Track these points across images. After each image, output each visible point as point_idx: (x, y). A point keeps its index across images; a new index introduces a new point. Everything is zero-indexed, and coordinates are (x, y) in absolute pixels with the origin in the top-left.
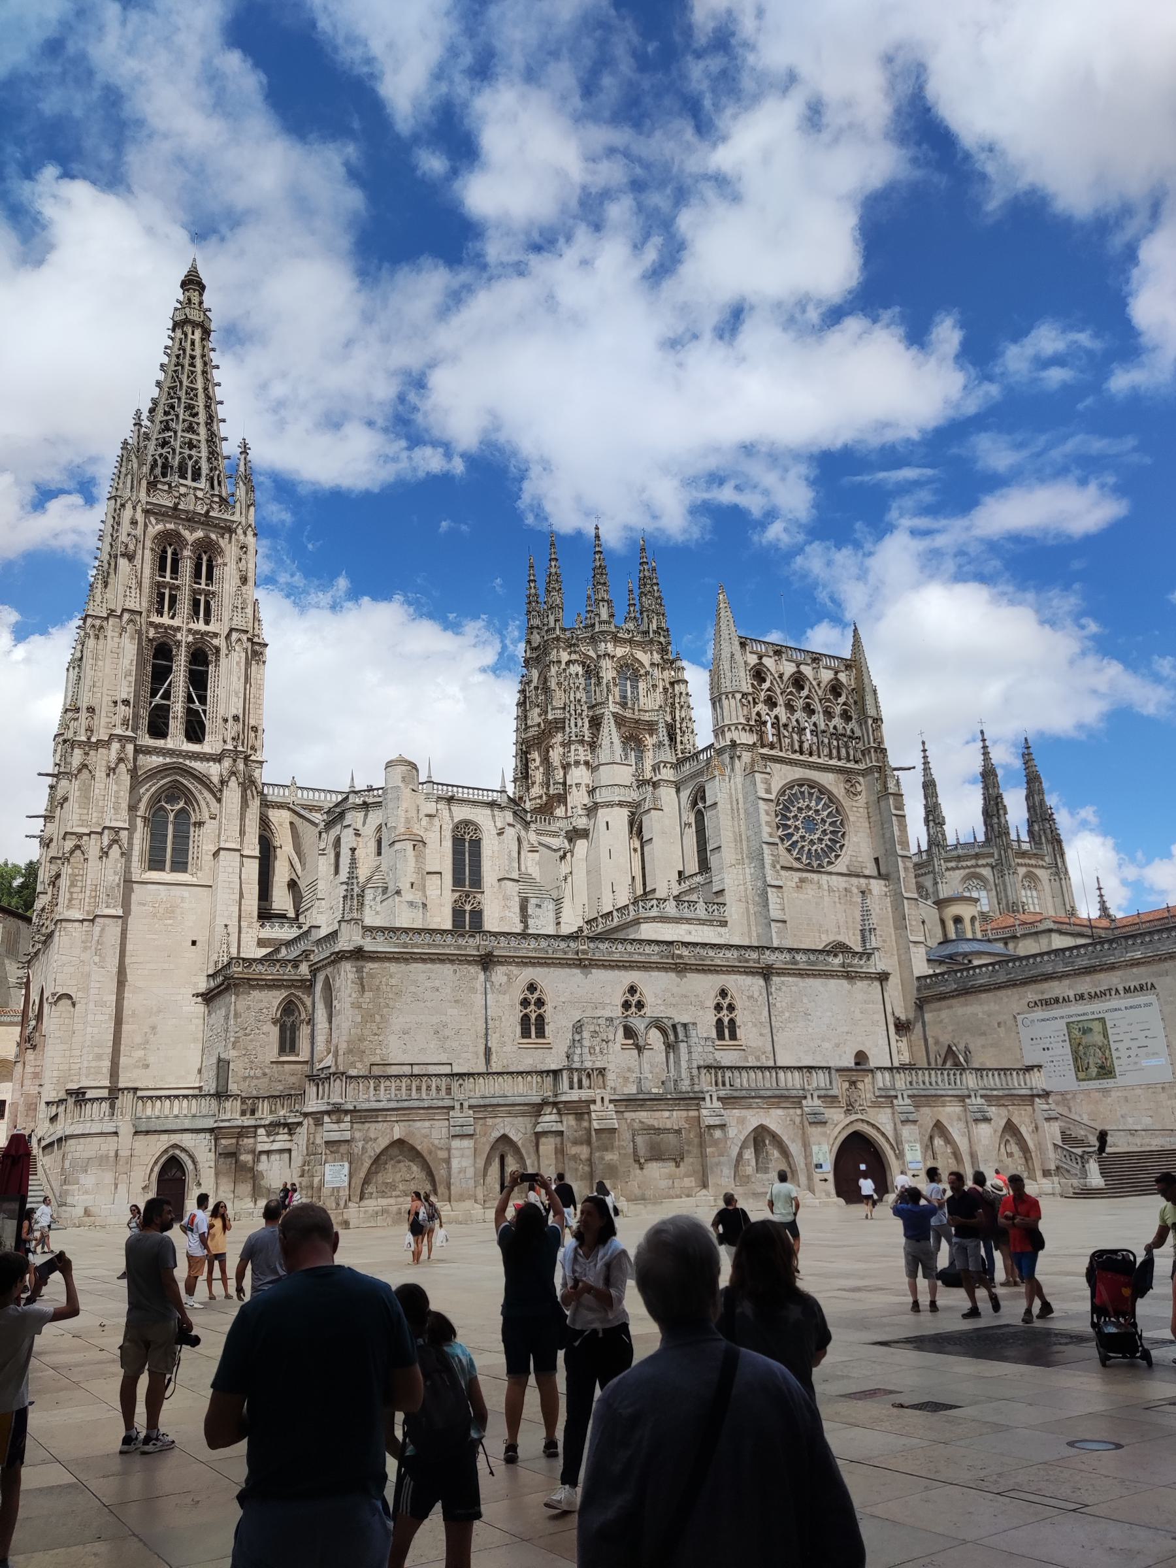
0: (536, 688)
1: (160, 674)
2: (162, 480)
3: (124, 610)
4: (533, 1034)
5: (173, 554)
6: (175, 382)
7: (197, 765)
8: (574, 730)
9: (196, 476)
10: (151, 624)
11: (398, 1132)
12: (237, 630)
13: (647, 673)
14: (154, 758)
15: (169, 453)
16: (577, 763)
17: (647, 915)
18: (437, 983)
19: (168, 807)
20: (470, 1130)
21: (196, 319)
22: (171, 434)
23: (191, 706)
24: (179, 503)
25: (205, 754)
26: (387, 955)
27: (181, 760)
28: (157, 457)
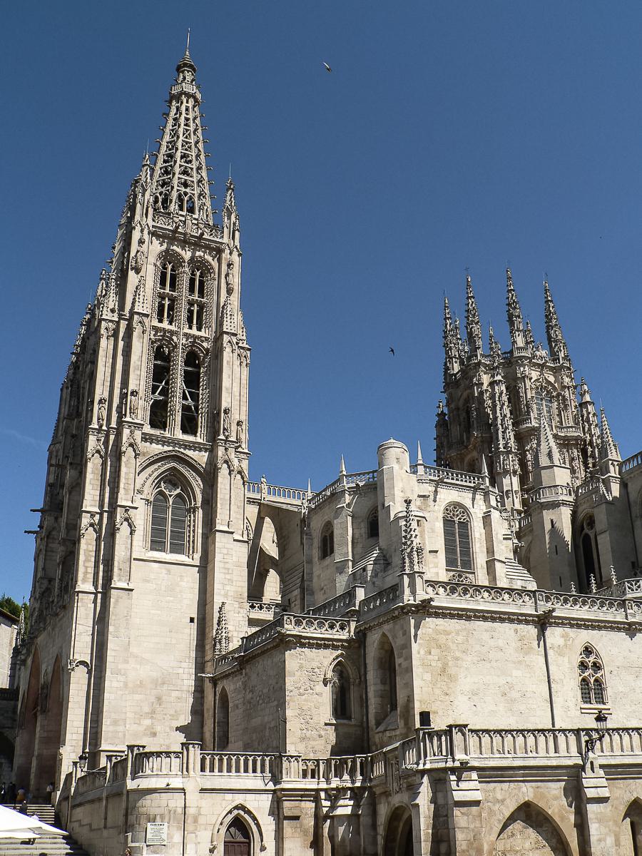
0: (458, 409)
1: (161, 373)
2: (162, 210)
3: (132, 313)
4: (593, 701)
6: (172, 137)
7: (190, 453)
8: (501, 442)
9: (191, 210)
10: (154, 328)
11: (527, 792)
12: (227, 333)
13: (559, 395)
15: (168, 190)
16: (506, 472)
17: (635, 595)
18: (501, 643)
19: (167, 493)
20: (604, 793)
27: (177, 449)
28: (158, 195)
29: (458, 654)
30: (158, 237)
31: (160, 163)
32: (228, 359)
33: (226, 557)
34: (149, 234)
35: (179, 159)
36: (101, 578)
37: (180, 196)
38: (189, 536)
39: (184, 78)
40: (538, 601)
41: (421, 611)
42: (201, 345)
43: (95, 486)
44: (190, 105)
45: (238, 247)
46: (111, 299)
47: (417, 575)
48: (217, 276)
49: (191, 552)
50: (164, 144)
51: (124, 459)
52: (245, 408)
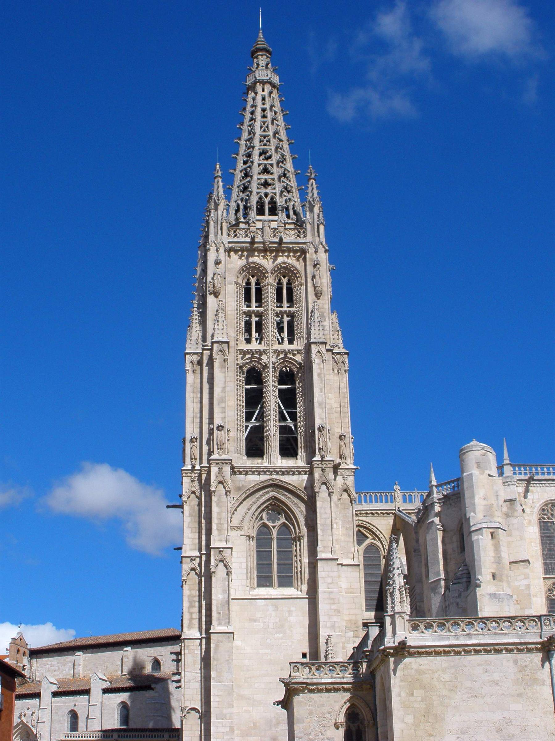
3: (213, 343)
5: (256, 284)
10: (241, 351)
14: (251, 477)
15: (247, 196)
19: (270, 524)
21: (265, 78)
22: (249, 179)
23: (283, 424)
24: (254, 237)
25: (298, 467)
26: (437, 649)
27: (275, 477)
28: (239, 202)
29: (445, 693)
30: (236, 251)
31: (240, 165)
32: (319, 371)
33: (330, 586)
34: (225, 251)
35: (257, 157)
36: (204, 623)
37: (261, 198)
38: (297, 567)
39: (258, 65)
40: (544, 627)
41: (400, 653)
42: (294, 360)
43: (194, 530)
44: (266, 93)
45: (324, 243)
46: (194, 330)
47: (397, 616)
48: (303, 280)
49: (299, 583)
50: (243, 142)
51: (214, 499)
52: (348, 420)
